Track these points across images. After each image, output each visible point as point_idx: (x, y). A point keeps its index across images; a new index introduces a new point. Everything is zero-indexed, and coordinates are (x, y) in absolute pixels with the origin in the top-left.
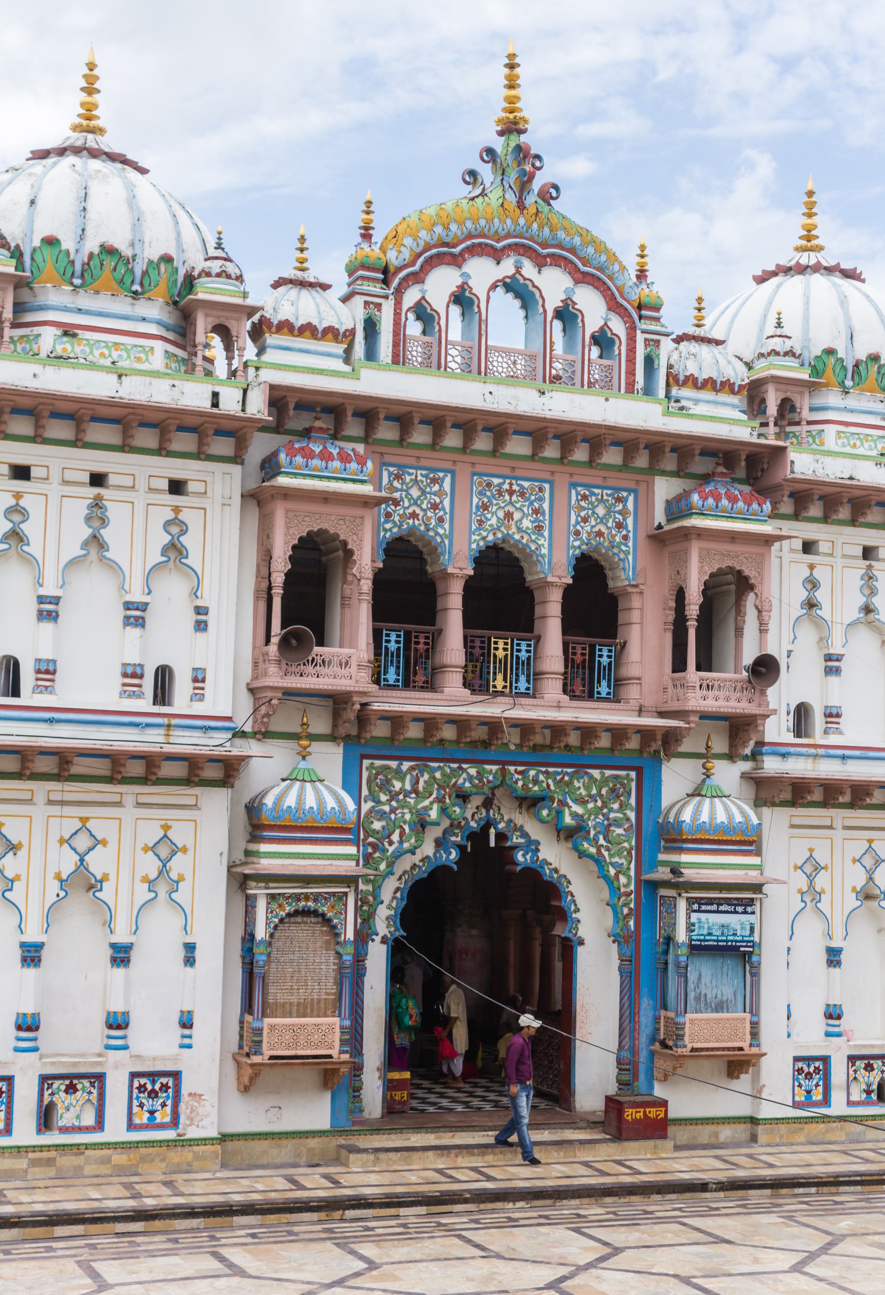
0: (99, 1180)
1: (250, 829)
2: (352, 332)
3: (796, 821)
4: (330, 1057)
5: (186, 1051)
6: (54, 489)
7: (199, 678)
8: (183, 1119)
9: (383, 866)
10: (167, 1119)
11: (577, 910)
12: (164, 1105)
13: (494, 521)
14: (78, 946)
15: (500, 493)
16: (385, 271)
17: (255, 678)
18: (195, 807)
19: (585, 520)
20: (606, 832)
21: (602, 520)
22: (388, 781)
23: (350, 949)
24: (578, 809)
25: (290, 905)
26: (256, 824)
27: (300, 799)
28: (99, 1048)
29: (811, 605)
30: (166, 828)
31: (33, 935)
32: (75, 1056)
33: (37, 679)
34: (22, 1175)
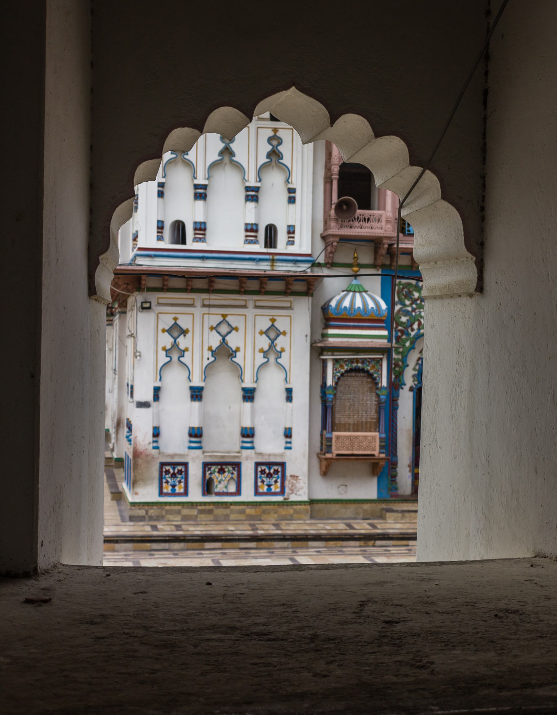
0: (238, 521)
1: (324, 321)
4: (373, 455)
5: (288, 451)
7: (291, 231)
8: (287, 490)
10: (278, 490)
12: (276, 482)
14: (224, 390)
17: (325, 229)
18: (290, 308)
23: (385, 392)
25: (347, 365)
26: (327, 318)
27: (352, 302)
28: (238, 449)
30: (273, 320)
31: (197, 382)
32: (224, 452)
33: (195, 234)
34: (195, 518)
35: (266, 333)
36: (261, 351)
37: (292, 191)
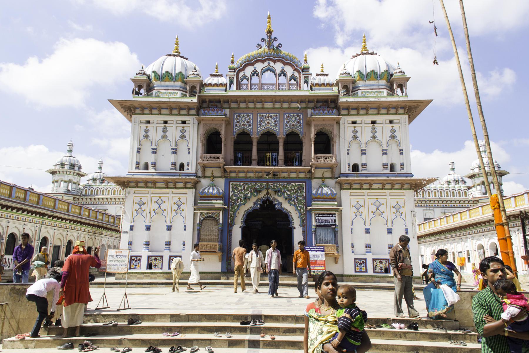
2: (226, 84)
3: (352, 194)
6: (155, 125)
7: (188, 165)
9: (236, 208)
11: (293, 220)
13: (264, 124)
15: (265, 117)
16: (235, 70)
18: (186, 194)
19: (289, 122)
20: (297, 199)
22: (237, 188)
24: (289, 193)
29: (355, 137)
30: (179, 198)
36: (174, 210)
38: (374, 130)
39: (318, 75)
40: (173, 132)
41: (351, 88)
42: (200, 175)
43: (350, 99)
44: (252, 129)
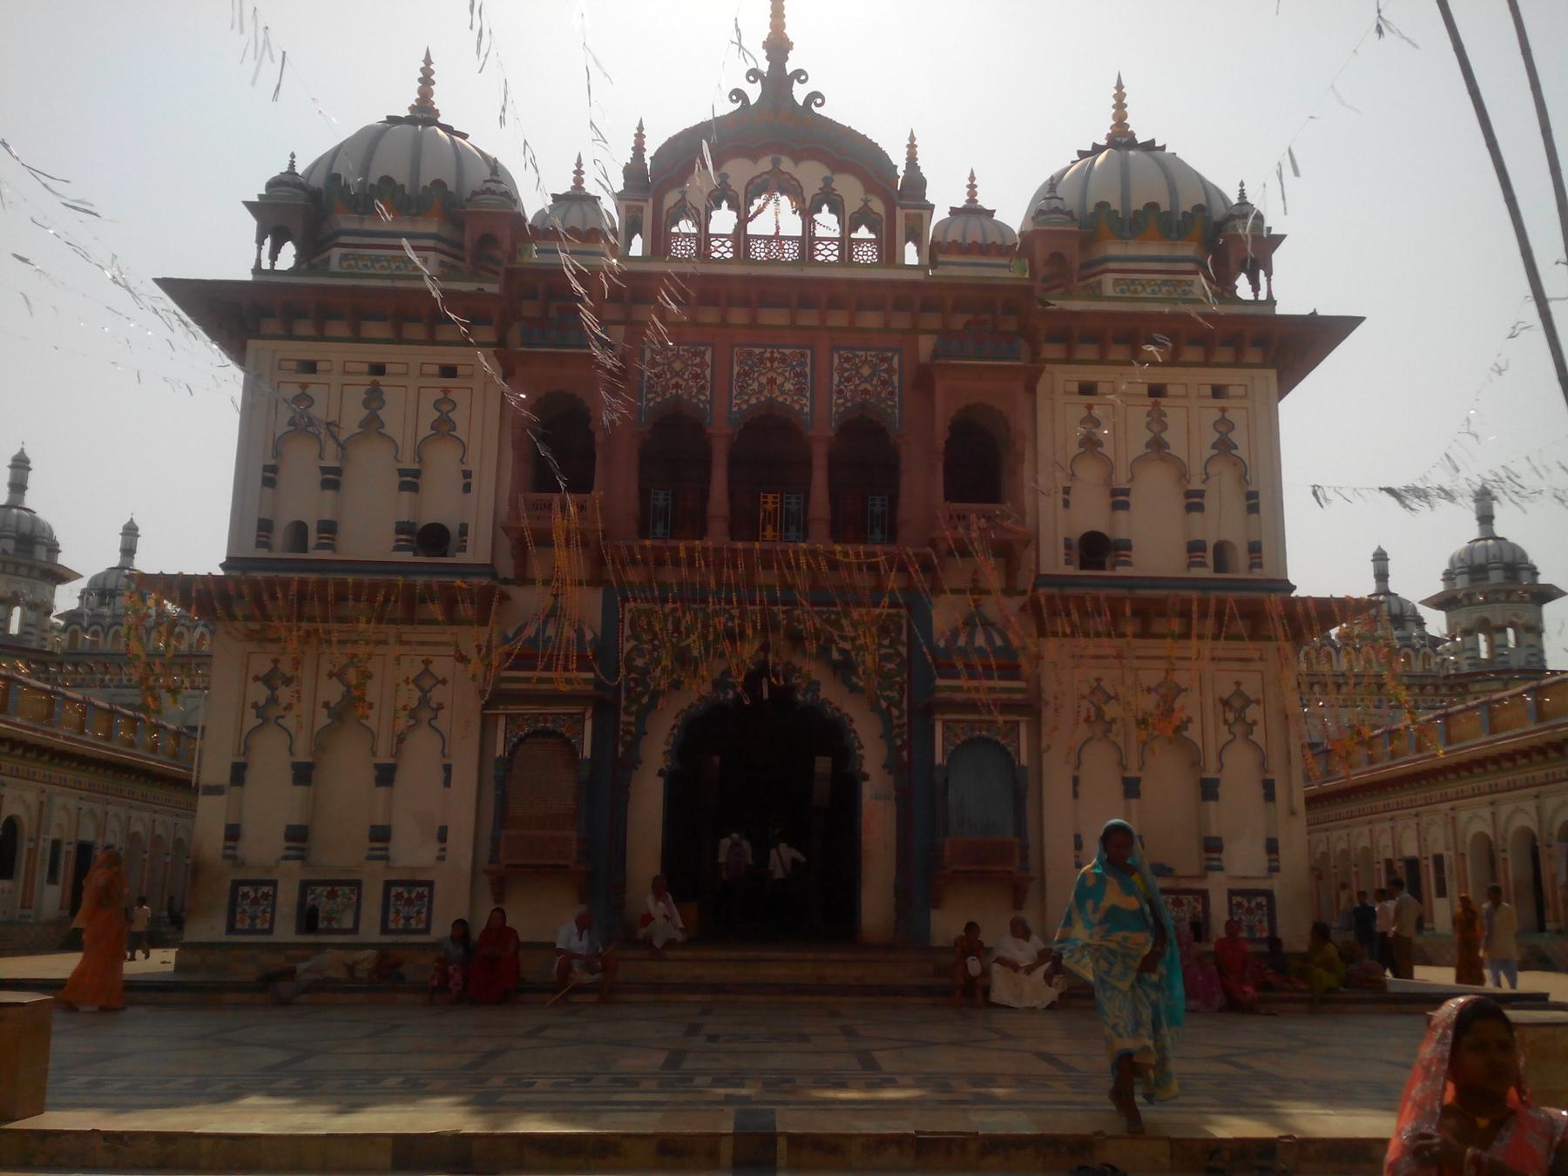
4: (567, 867)
9: (645, 700)
12: (419, 912)
13: (755, 386)
15: (762, 361)
19: (848, 380)
21: (867, 380)
24: (847, 646)
30: (427, 662)
31: (302, 758)
35: (416, 681)
37: (467, 474)
38: (1157, 419)
39: (954, 211)
40: (407, 410)
41: (1076, 265)
42: (510, 575)
43: (1076, 305)
44: (710, 402)
